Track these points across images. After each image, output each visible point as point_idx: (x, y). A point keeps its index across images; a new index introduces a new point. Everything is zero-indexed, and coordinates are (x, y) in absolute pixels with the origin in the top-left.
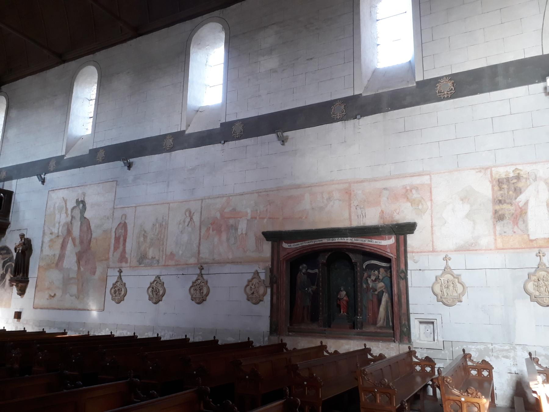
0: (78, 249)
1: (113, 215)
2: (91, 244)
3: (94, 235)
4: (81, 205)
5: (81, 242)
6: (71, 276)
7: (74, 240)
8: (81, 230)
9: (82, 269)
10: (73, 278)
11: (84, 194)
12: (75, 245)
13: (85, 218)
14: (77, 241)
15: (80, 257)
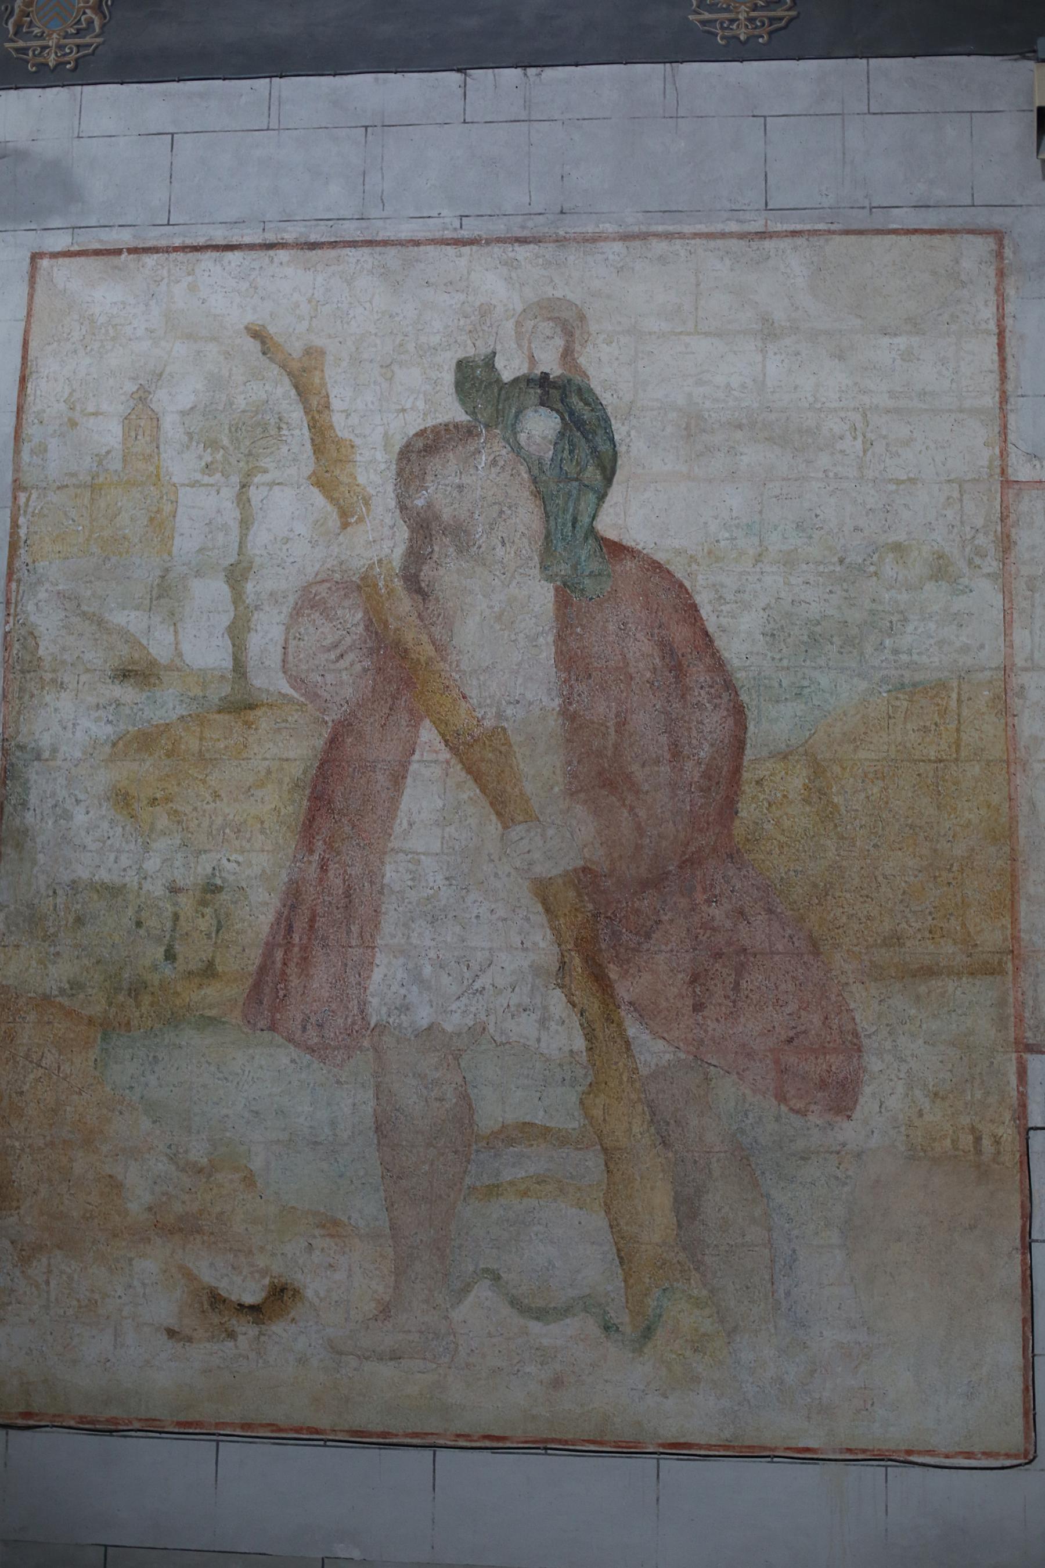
0: (565, 838)
1: (1006, 544)
2: (747, 811)
3: (773, 724)
4: (540, 426)
5: (601, 775)
6: (493, 1112)
7: (482, 759)
8: (572, 662)
9: (652, 1050)
10: (528, 1132)
11: (570, 325)
12: (502, 802)
13: (616, 550)
14: (540, 769)
15: (597, 931)
